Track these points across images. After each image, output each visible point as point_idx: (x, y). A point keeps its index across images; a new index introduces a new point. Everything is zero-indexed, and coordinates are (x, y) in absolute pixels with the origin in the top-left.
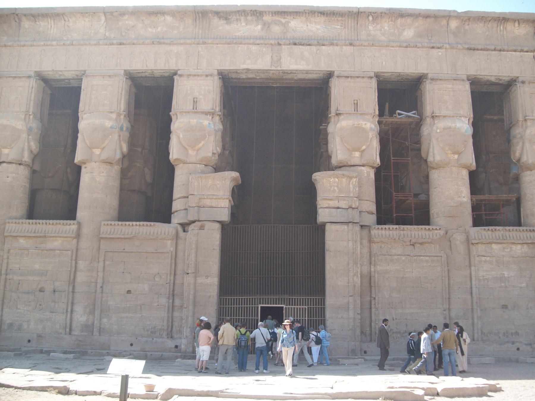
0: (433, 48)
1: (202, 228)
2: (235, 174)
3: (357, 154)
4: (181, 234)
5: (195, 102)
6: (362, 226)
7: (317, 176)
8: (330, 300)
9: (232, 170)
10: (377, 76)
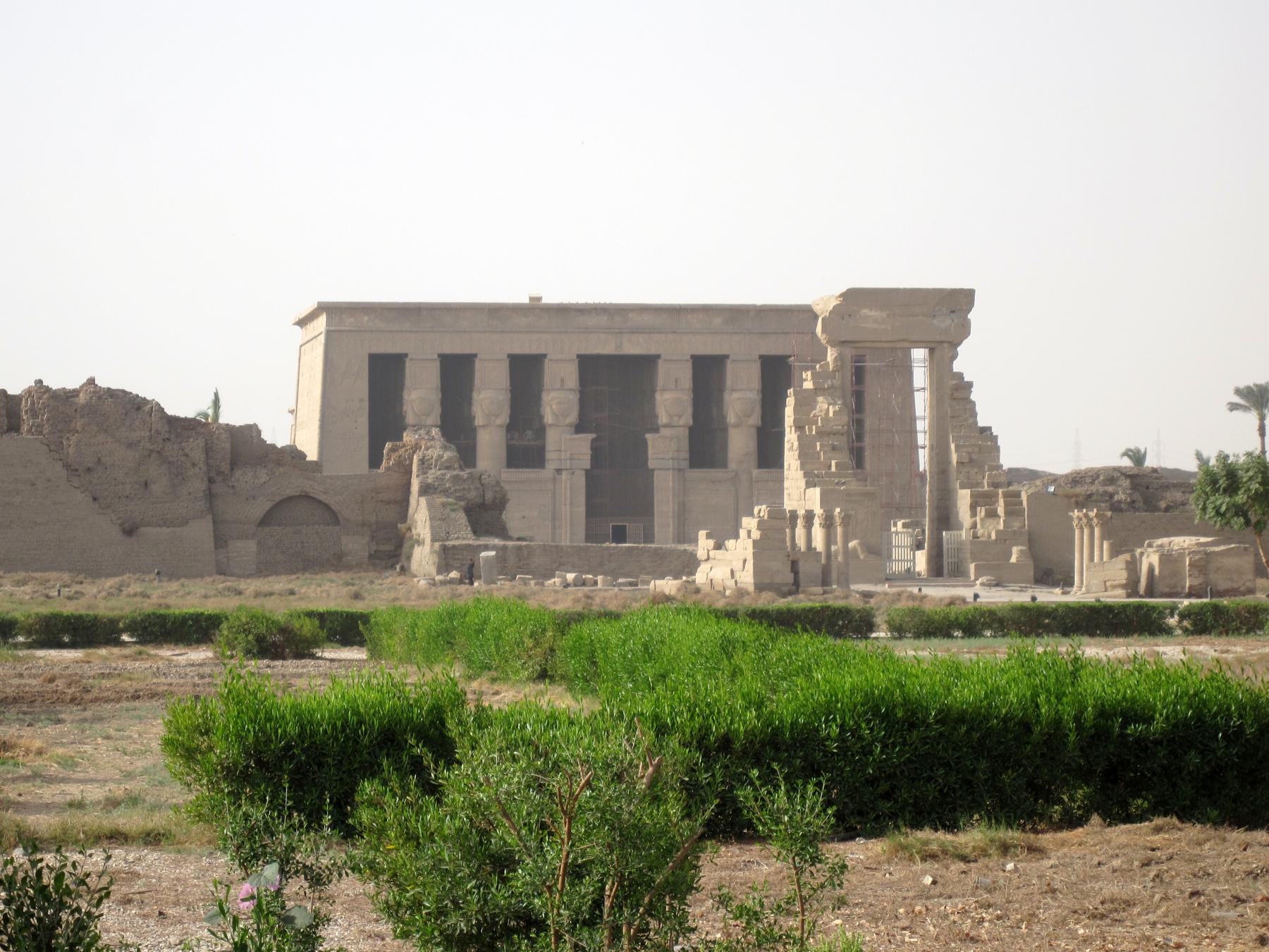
0: (735, 333)
1: (573, 473)
2: (593, 436)
3: (676, 419)
4: (558, 477)
5: (562, 380)
6: (679, 470)
7: (648, 436)
8: (657, 521)
9: (591, 432)
10: (693, 357)
